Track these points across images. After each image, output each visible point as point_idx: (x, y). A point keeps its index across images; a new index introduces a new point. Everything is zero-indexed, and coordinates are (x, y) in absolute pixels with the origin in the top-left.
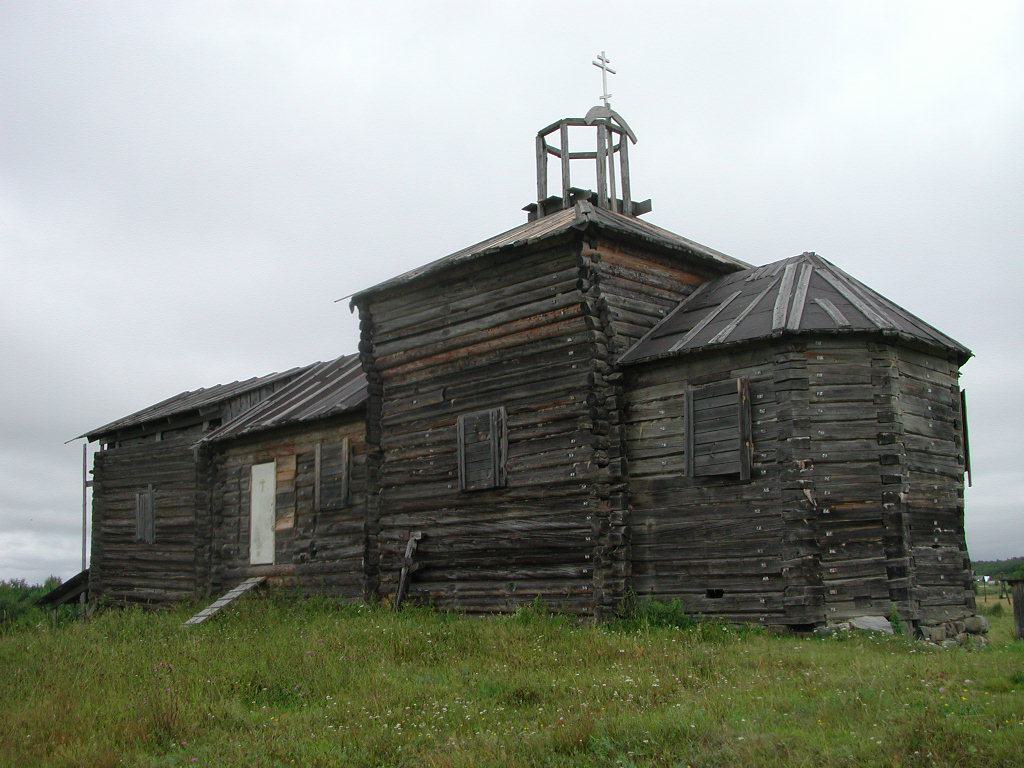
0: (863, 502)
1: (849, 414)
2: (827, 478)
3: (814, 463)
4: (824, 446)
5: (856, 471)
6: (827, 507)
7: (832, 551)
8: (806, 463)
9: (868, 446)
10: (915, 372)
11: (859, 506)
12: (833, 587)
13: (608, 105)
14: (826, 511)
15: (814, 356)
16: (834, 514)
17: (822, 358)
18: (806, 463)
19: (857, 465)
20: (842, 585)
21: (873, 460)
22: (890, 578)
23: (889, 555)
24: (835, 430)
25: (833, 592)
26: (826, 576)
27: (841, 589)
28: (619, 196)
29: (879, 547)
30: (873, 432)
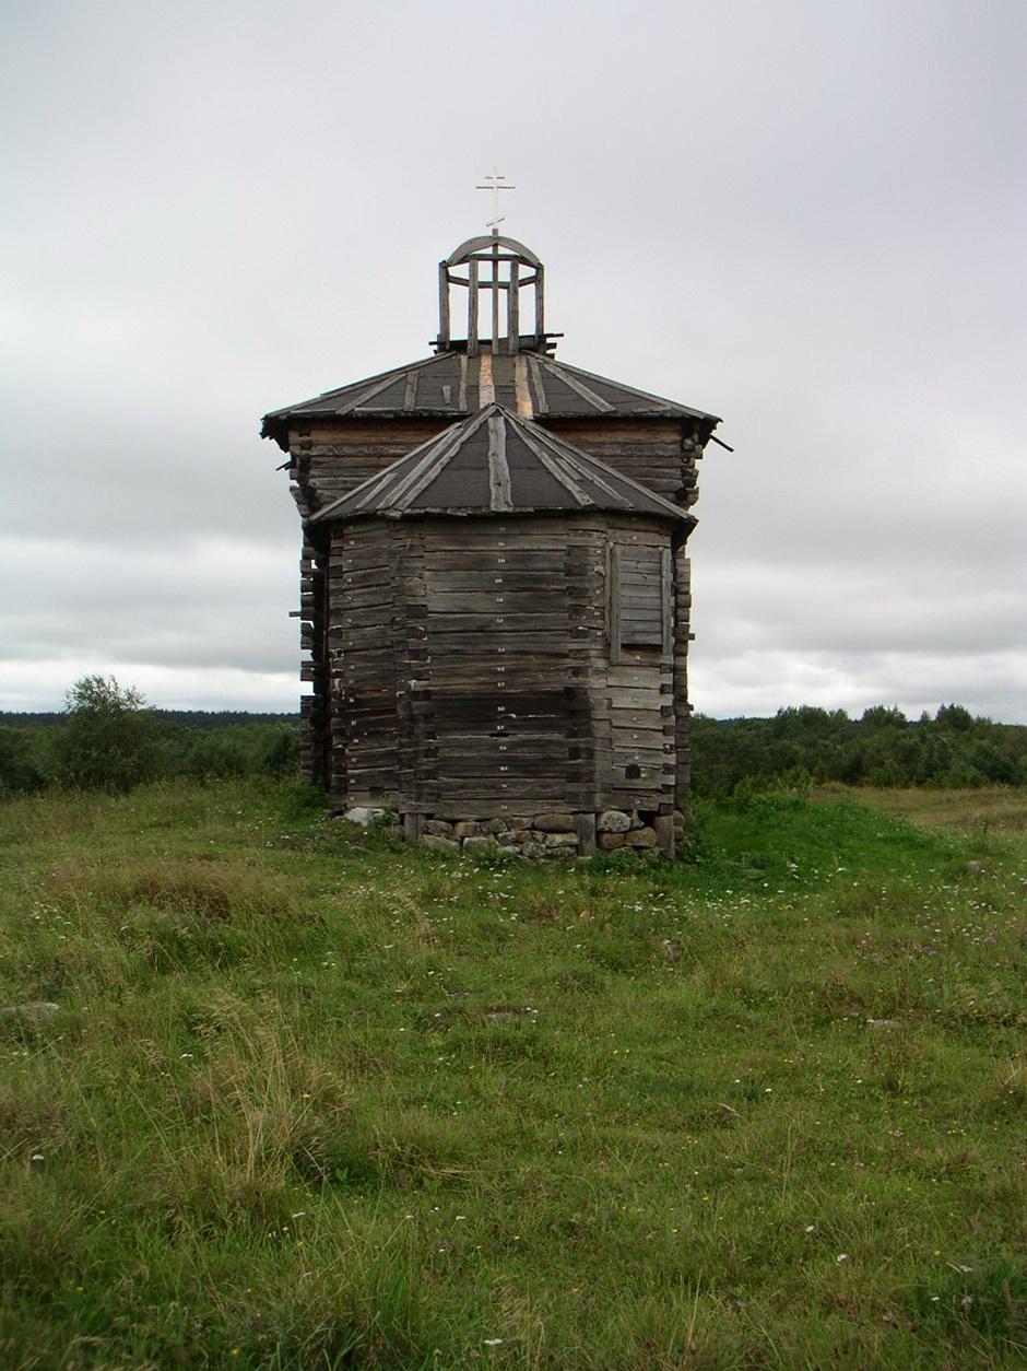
0: (379, 691)
1: (371, 599)
2: (353, 667)
3: (345, 652)
4: (352, 634)
5: (375, 659)
6: (352, 695)
7: (356, 741)
8: (339, 652)
9: (384, 632)
10: (466, 543)
11: (376, 695)
12: (353, 776)
13: (495, 231)
14: (352, 700)
15: (347, 542)
16: (359, 703)
17: (353, 543)
18: (339, 652)
19: (374, 653)
20: (359, 775)
21: (389, 647)
22: (400, 769)
23: (402, 745)
24: (359, 617)
25: (352, 781)
26: (349, 766)
27: (359, 778)
28: (503, 333)
29: (395, 737)
30: (387, 617)
